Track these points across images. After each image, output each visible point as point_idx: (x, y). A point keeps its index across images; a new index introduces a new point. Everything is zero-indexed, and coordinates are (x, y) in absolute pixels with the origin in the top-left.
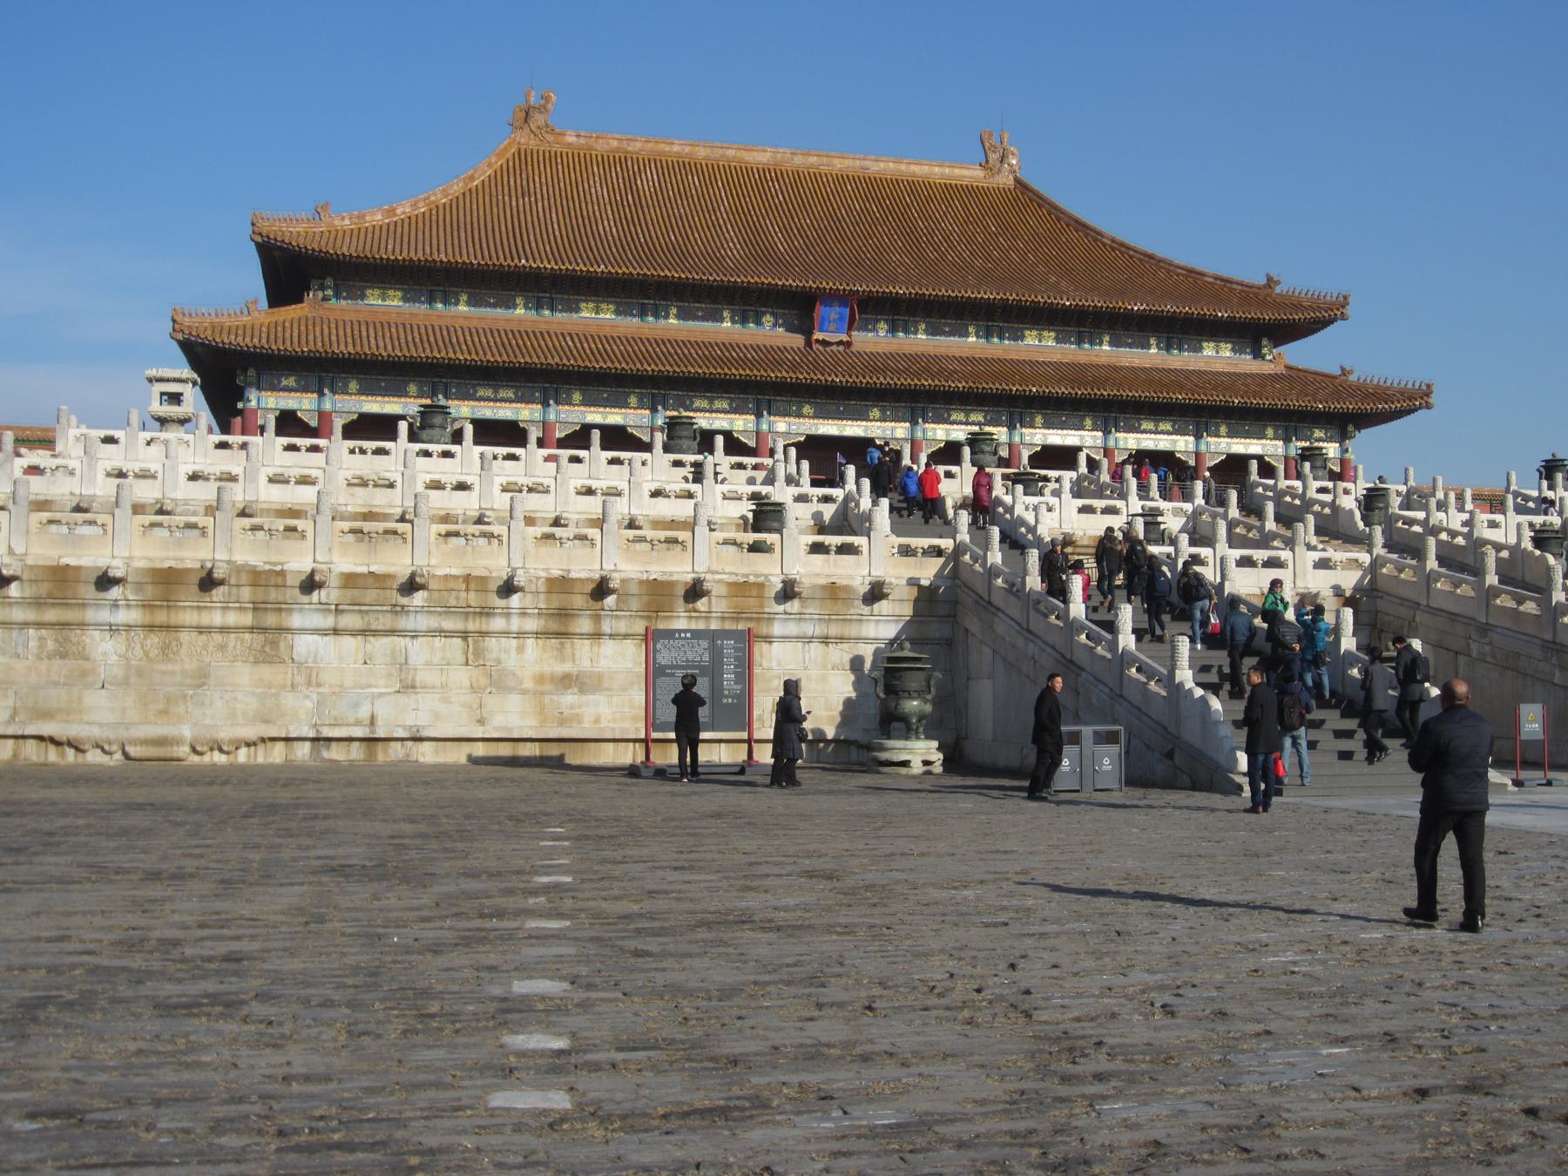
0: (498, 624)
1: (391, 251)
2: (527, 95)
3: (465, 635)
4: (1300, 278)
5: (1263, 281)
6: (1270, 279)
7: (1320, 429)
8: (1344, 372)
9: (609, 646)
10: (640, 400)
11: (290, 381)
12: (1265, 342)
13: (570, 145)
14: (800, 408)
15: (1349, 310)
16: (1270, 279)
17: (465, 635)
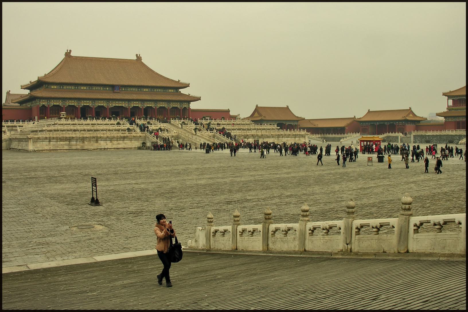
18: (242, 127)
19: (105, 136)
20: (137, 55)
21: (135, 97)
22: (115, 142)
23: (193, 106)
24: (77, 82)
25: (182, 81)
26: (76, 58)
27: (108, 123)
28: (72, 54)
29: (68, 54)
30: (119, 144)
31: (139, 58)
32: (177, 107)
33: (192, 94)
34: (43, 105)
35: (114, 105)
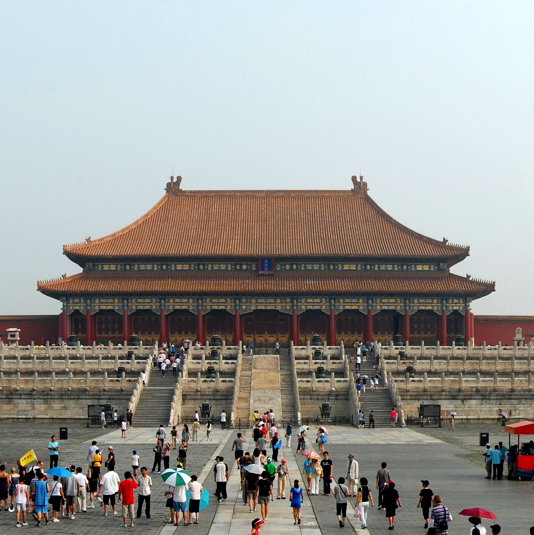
0: (50, 397)
1: (110, 252)
2: (172, 178)
3: (44, 399)
4: (456, 240)
5: (442, 240)
6: (444, 239)
7: (456, 299)
8: (468, 277)
9: (71, 401)
10: (193, 300)
11: (77, 300)
12: (441, 265)
13: (187, 196)
14: (251, 300)
15: (470, 253)
16: (444, 239)
17: (44, 399)
18: (484, 367)
19: (30, 386)
20: (354, 178)
21: (309, 285)
22: (57, 405)
23: (479, 307)
24: (161, 251)
25: (452, 241)
26: (194, 194)
27: (113, 353)
28: (183, 186)
29: (173, 188)
30: (65, 408)
31: (360, 187)
32: (431, 312)
33: (474, 276)
34: (77, 312)
35: (253, 308)
